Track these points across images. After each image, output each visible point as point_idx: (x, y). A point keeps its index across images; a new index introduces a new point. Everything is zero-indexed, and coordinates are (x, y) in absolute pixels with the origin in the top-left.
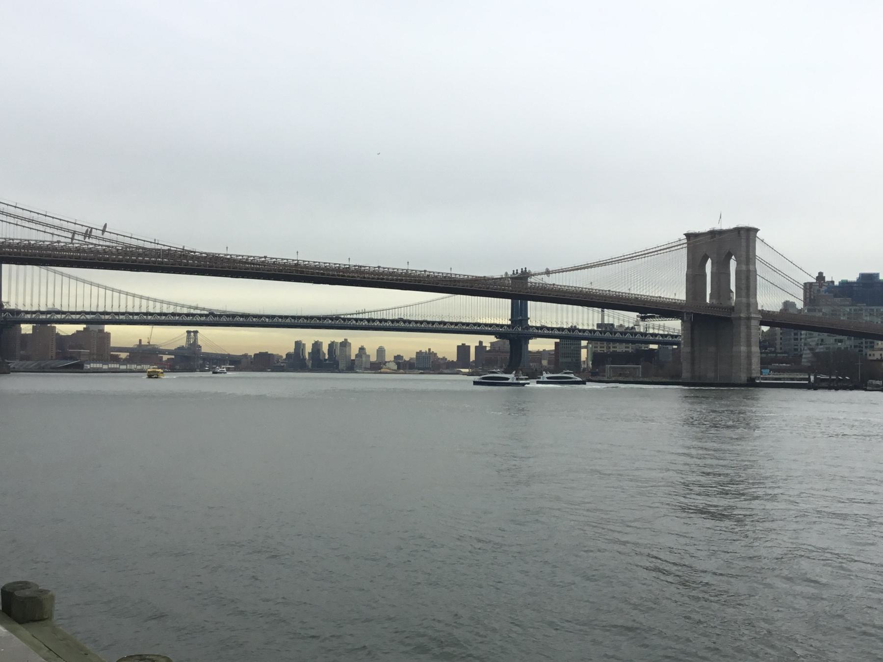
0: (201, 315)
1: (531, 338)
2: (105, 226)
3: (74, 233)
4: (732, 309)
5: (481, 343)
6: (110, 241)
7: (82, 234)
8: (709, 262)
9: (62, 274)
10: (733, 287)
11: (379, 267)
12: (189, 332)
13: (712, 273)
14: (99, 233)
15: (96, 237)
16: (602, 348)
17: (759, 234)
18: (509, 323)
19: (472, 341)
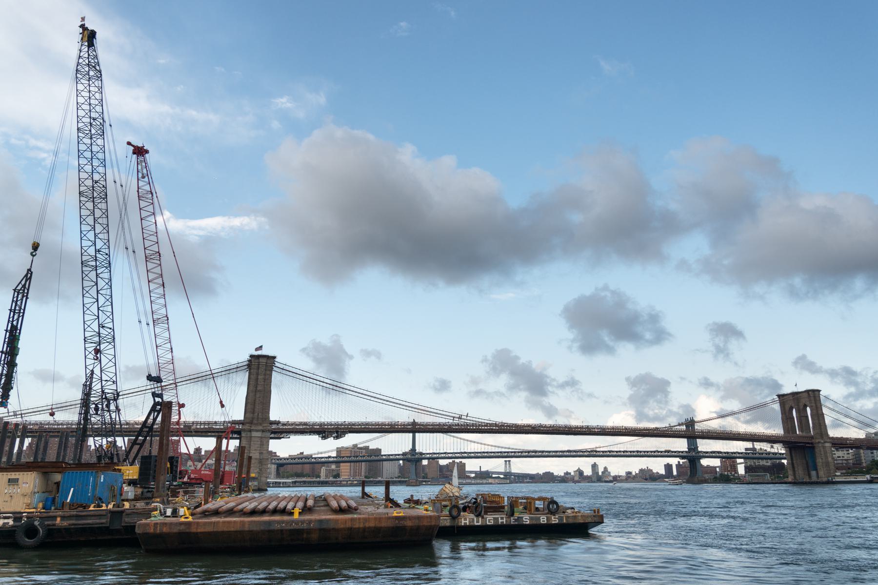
0: (512, 452)
1: (700, 459)
2: (467, 414)
3: (454, 417)
4: (812, 437)
5: (679, 462)
6: (470, 420)
7: (456, 418)
8: (794, 410)
9: (454, 437)
10: (811, 425)
11: (598, 426)
12: (506, 461)
13: (797, 417)
14: (465, 417)
15: (464, 419)
16: (750, 463)
17: (821, 393)
18: (687, 450)
19: (674, 461)
